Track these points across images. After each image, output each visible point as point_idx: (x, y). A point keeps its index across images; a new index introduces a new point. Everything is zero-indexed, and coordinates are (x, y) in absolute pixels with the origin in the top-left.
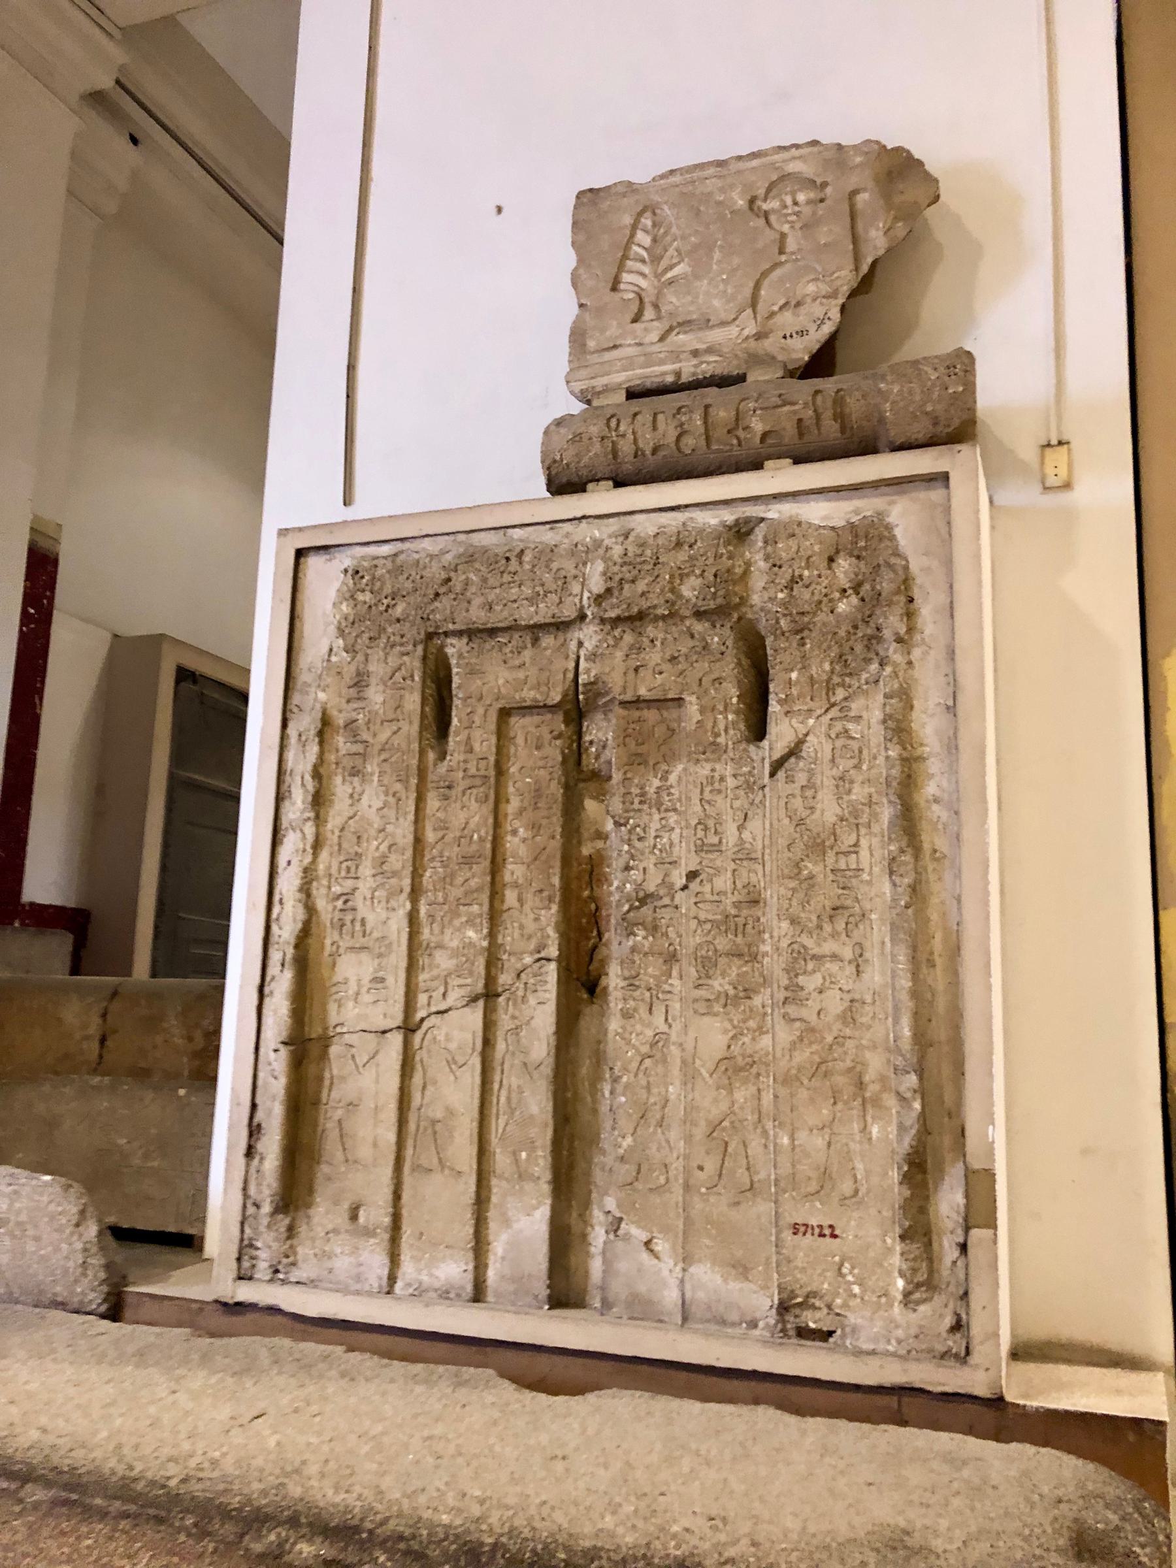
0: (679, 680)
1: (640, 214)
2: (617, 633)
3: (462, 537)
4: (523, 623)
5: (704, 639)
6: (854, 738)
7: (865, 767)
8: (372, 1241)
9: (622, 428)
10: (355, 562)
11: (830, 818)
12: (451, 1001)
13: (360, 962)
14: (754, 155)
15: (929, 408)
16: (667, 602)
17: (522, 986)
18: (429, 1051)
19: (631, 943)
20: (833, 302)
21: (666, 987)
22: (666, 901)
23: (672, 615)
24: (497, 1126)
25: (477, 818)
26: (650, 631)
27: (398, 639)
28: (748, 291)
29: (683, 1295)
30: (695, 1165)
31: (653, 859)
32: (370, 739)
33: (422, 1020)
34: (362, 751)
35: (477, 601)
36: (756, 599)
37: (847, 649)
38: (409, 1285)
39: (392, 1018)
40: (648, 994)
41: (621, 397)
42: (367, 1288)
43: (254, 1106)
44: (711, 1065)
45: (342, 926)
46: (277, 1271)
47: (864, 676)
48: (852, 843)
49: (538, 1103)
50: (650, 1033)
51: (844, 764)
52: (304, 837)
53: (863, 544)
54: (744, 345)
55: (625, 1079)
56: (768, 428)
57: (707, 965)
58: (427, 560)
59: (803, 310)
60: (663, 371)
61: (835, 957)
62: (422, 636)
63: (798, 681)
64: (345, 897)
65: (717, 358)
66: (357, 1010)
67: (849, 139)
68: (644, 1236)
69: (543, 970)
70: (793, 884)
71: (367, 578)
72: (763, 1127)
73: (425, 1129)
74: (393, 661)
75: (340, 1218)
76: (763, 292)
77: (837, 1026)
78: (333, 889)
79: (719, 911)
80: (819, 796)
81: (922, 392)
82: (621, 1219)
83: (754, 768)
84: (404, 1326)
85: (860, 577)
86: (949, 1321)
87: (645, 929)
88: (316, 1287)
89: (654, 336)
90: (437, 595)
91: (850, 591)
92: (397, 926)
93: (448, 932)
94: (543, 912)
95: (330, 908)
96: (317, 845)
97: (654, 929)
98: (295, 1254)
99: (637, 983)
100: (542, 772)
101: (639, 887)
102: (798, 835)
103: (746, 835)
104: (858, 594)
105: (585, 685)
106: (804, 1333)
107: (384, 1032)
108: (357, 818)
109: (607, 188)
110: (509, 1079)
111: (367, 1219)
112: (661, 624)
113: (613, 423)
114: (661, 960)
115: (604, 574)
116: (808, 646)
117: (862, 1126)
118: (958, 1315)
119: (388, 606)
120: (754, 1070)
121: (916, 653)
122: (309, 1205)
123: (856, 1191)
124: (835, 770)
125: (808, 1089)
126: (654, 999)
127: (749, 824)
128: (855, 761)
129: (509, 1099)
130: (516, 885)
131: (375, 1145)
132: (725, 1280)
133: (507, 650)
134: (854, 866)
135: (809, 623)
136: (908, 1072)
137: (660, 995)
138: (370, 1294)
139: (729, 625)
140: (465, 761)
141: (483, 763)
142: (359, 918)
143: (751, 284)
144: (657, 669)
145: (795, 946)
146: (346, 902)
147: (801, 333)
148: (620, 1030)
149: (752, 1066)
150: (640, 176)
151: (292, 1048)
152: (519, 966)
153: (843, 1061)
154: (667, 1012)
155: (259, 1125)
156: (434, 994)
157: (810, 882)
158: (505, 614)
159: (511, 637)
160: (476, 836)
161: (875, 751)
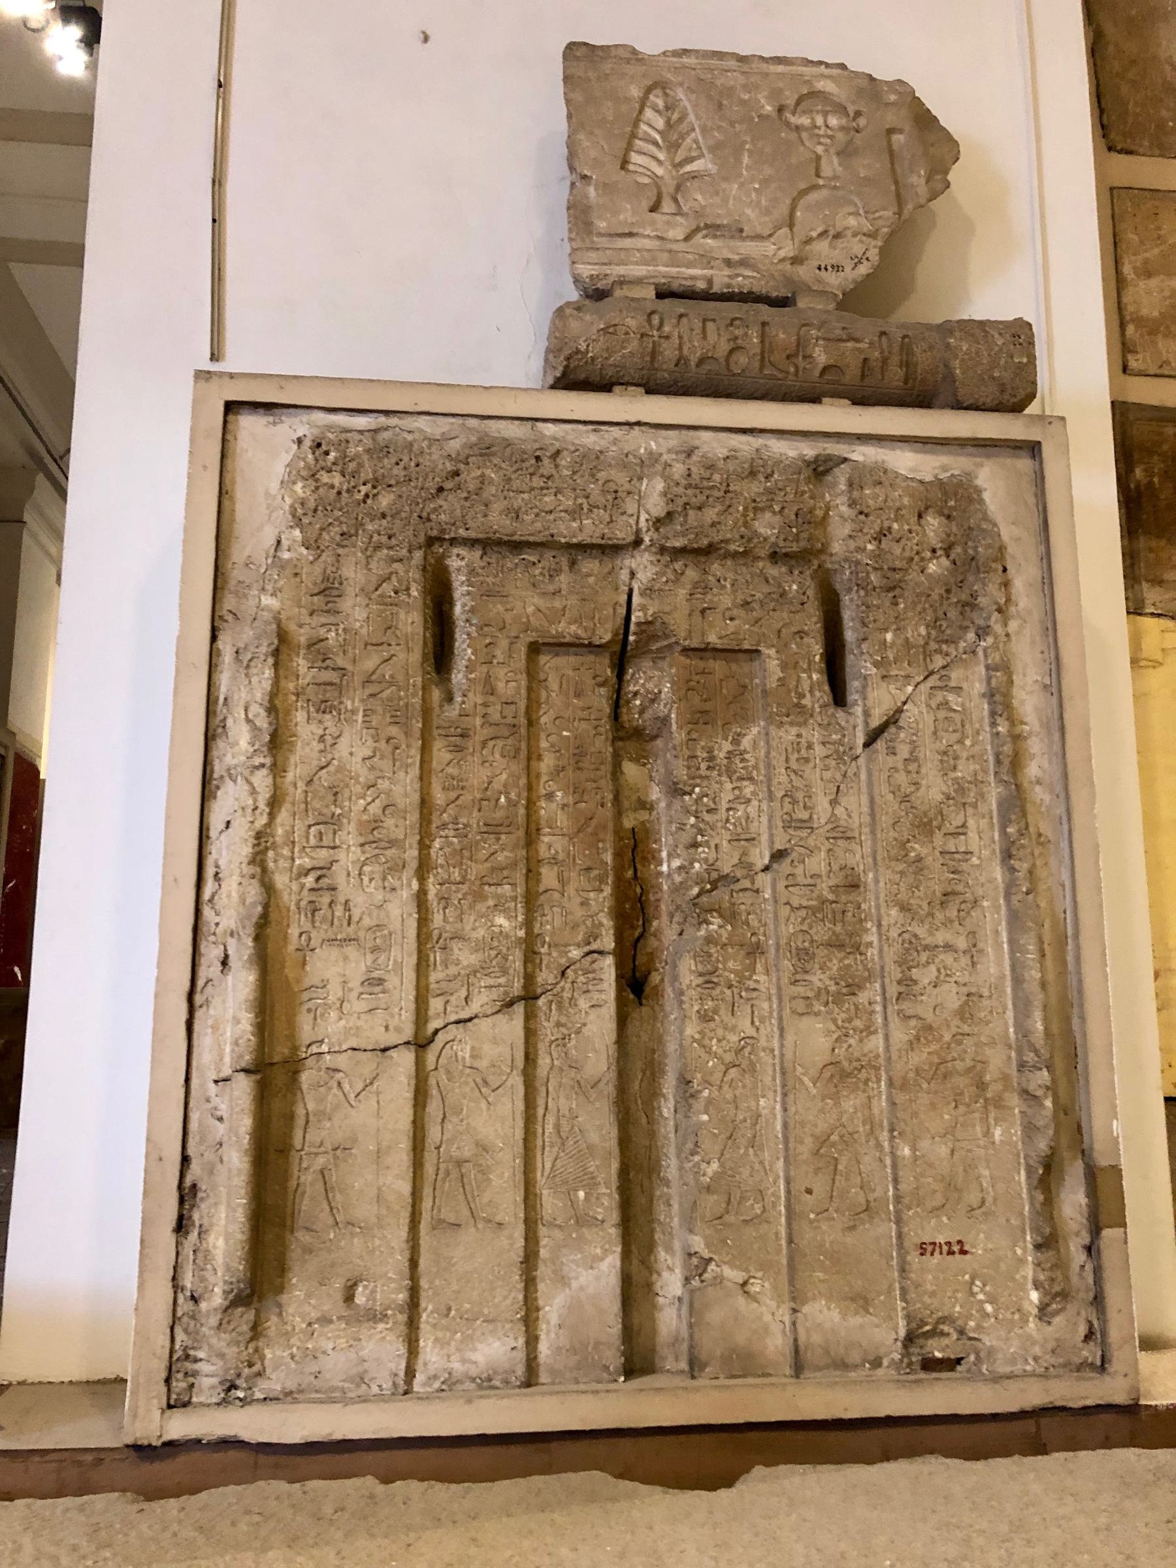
0: (755, 629)
1: (649, 90)
2: (678, 566)
3: (473, 422)
4: (563, 540)
5: (780, 586)
6: (955, 711)
7: (968, 742)
8: (381, 1326)
9: (667, 329)
10: (316, 431)
11: (935, 795)
12: (475, 1007)
13: (346, 958)
14: (779, 60)
15: (996, 374)
16: (742, 537)
17: (568, 986)
18: (448, 1072)
19: (702, 933)
20: (873, 243)
21: (752, 985)
22: (746, 883)
23: (745, 553)
24: (545, 1162)
25: (504, 776)
26: (716, 568)
27: (384, 539)
28: (783, 209)
29: (796, 1340)
30: (803, 1189)
31: (727, 836)
32: (349, 667)
33: (436, 1032)
34: (338, 681)
35: (497, 506)
36: (837, 547)
37: (940, 614)
38: (435, 1377)
39: (398, 1030)
40: (728, 992)
41: (651, 293)
42: (375, 1390)
43: (185, 1160)
44: (814, 1072)
45: (314, 911)
46: (233, 1386)
47: (962, 644)
48: (960, 824)
49: (598, 1127)
50: (734, 1038)
51: (947, 739)
52: (253, 792)
53: (952, 503)
54: (780, 267)
55: (706, 1093)
56: (832, 362)
57: (803, 957)
58: (425, 444)
59: (840, 243)
60: (695, 275)
61: (948, 947)
62: (422, 539)
63: (893, 643)
64: (319, 873)
65: (755, 274)
66: (343, 1022)
67: (884, 73)
68: (737, 1276)
69: (595, 966)
70: (901, 867)
71: (332, 455)
72: (876, 1138)
73: (448, 1173)
74: (378, 567)
75: (329, 1301)
76: (799, 214)
77: (956, 1022)
78: (298, 862)
79: (814, 895)
80: (923, 771)
81: (989, 355)
82: (711, 1259)
83: (844, 736)
84: (435, 1434)
85: (952, 538)
86: (1082, 1330)
87: (721, 916)
88: (296, 1401)
89: (678, 233)
90: (441, 489)
91: (939, 553)
92: (399, 911)
93: (469, 920)
94: (592, 895)
95: (295, 887)
96: (275, 803)
97: (731, 916)
98: (262, 1358)
99: (715, 980)
100: (584, 725)
101: (711, 867)
102: (903, 814)
103: (839, 811)
104: (948, 556)
105: (639, 624)
106: (930, 1365)
107: (384, 1050)
108: (331, 768)
109: (605, 49)
110: (558, 1101)
111: (372, 1296)
112: (729, 563)
113: (656, 320)
114: (742, 953)
115: (665, 494)
116: (902, 606)
117: (985, 1129)
118: (1090, 1323)
119: (367, 496)
120: (863, 1075)
121: (1013, 625)
122: (280, 1290)
123: (983, 1202)
124: (938, 743)
125: (928, 1093)
126: (737, 997)
127: (843, 800)
128: (956, 736)
129: (557, 1126)
130: (554, 861)
131: (379, 1198)
132: (844, 1317)
133: (537, 572)
134: (962, 850)
135: (900, 581)
136: (1041, 1069)
137: (743, 994)
138: (380, 1398)
139: (808, 573)
140: (485, 705)
141: (509, 711)
142: (342, 899)
143: (788, 202)
144: (728, 614)
145: (906, 936)
146: (318, 879)
147: (837, 268)
148: (697, 1036)
149: (860, 1070)
150: (649, 46)
151: (258, 1077)
152: (563, 961)
153: (963, 1060)
154: (753, 1012)
155: (194, 1186)
156: (453, 999)
157: (919, 864)
158: (538, 525)
159: (541, 556)
160: (503, 799)
161: (977, 726)
